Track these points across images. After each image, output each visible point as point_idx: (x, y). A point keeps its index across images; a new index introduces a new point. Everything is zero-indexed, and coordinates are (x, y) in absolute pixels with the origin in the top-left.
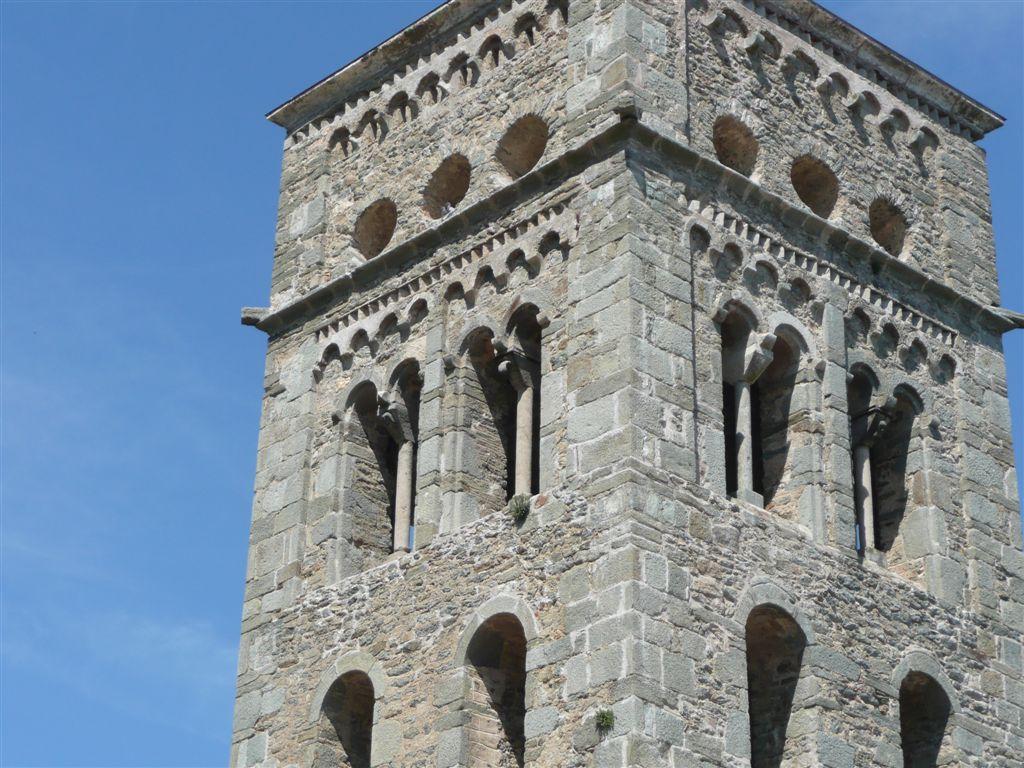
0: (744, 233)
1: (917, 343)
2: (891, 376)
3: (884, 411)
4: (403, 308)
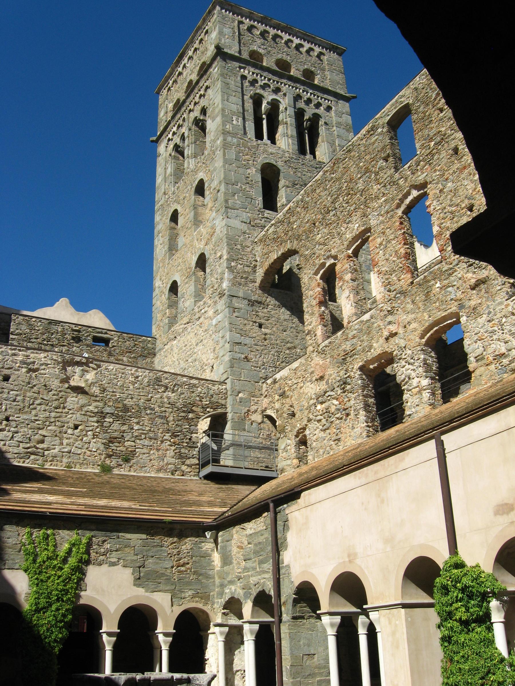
0: (259, 76)
1: (318, 102)
2: (309, 112)
3: (309, 120)
4: (181, 122)
